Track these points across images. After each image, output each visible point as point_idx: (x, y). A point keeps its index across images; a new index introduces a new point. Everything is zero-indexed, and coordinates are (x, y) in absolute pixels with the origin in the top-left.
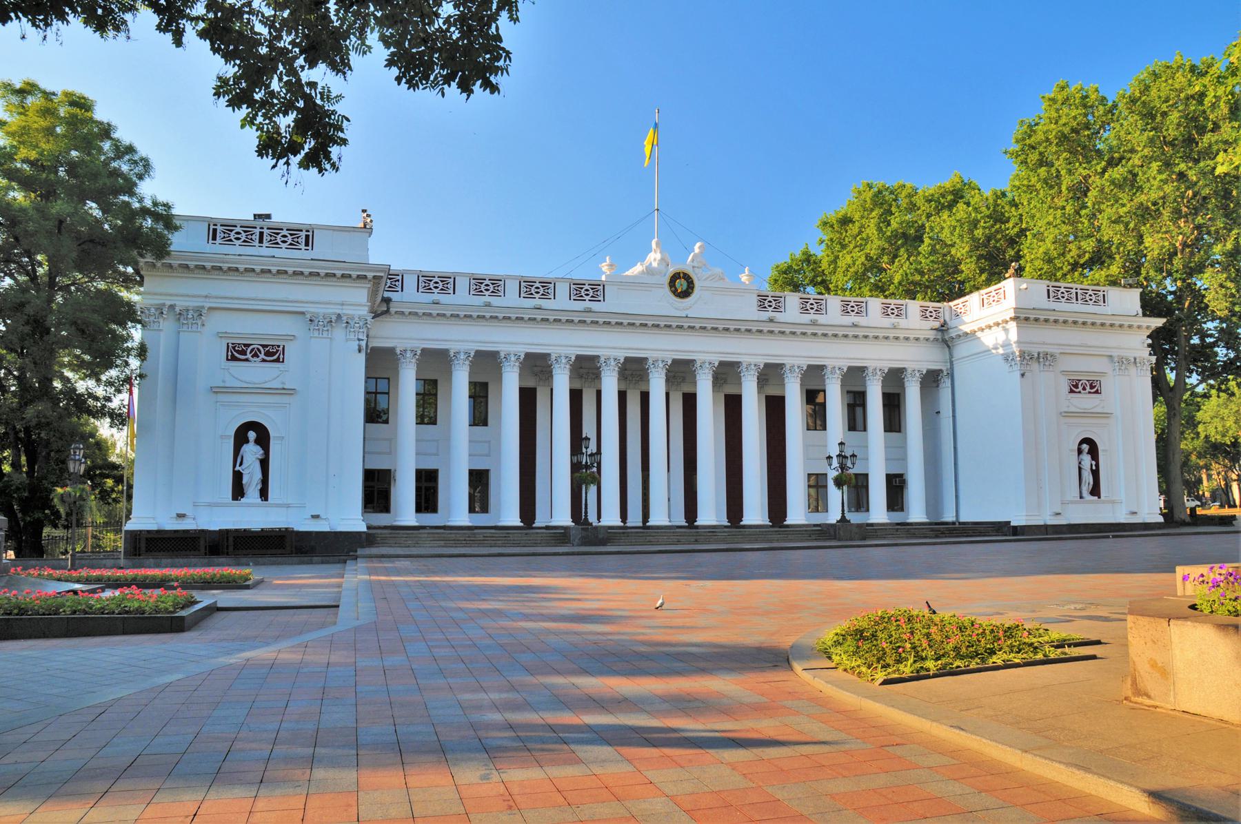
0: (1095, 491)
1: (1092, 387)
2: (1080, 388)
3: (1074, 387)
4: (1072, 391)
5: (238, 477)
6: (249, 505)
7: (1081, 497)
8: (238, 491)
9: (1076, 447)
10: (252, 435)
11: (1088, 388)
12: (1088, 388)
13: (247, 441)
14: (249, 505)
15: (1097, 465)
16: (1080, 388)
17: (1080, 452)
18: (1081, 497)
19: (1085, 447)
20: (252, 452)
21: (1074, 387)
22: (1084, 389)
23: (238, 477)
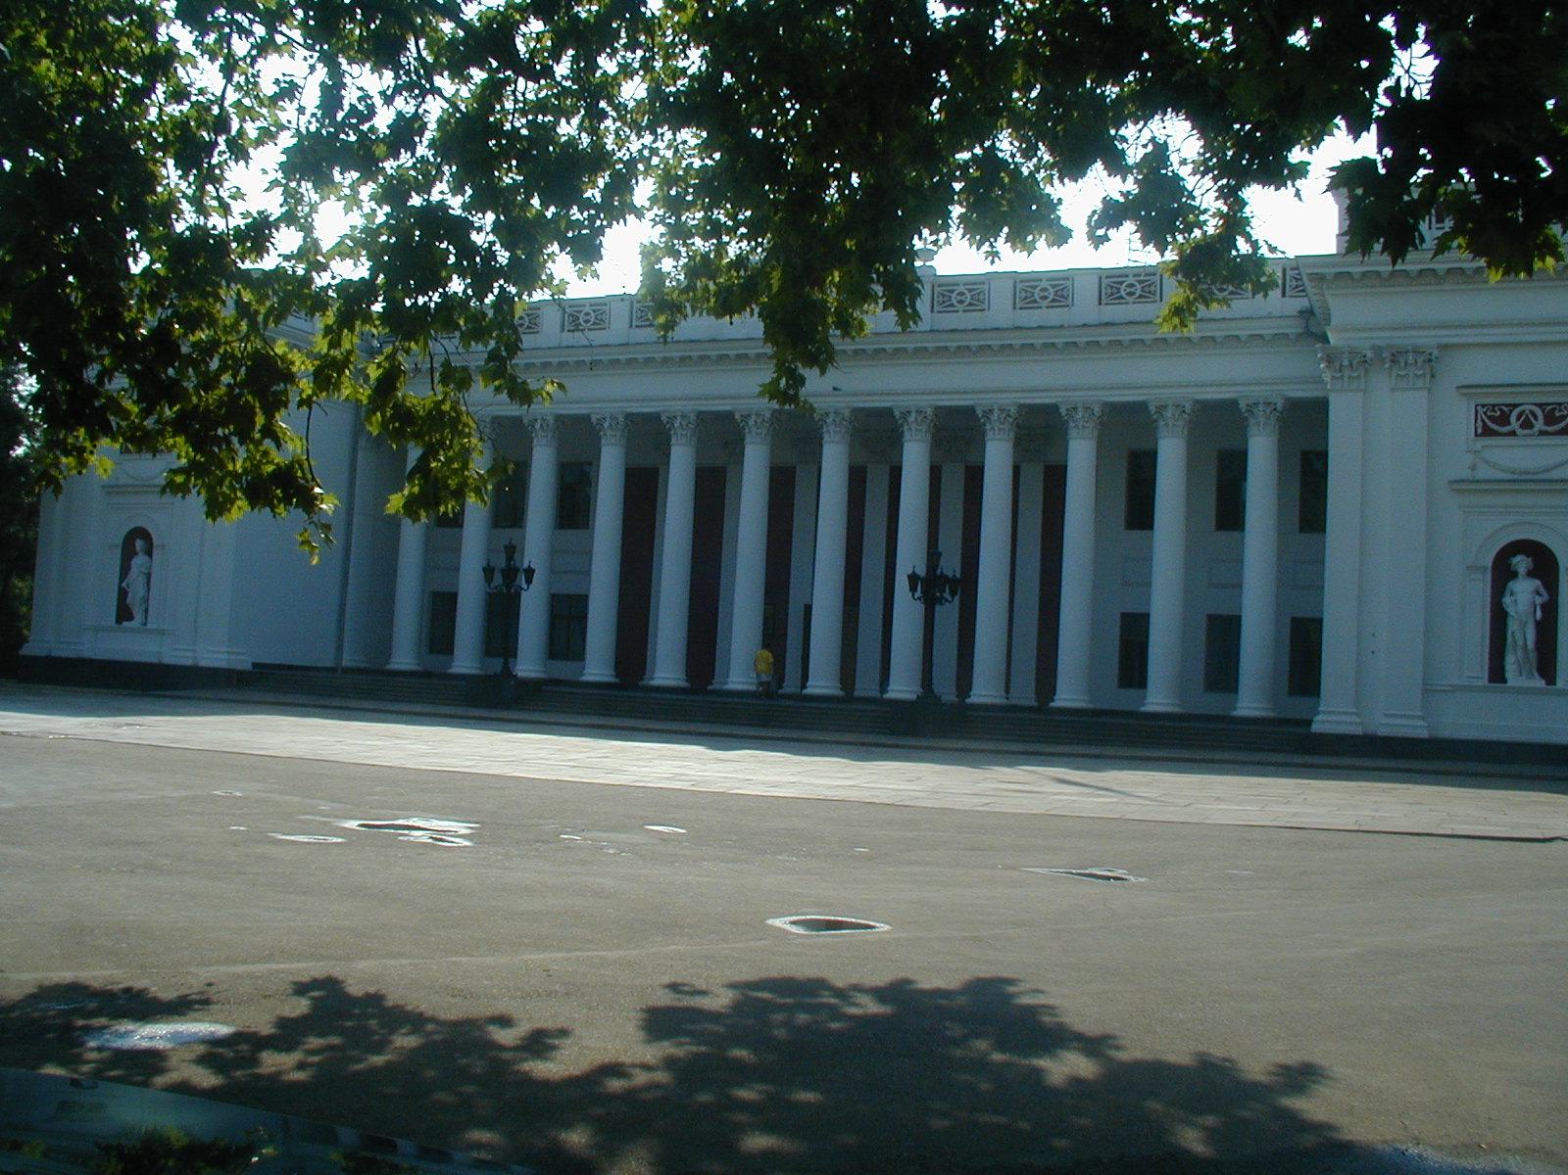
0: (1546, 664)
1: (1550, 419)
2: (1514, 424)
3: (1495, 421)
4: (1487, 432)
5: (123, 594)
6: (132, 630)
7: (1497, 674)
8: (124, 613)
9: (1489, 563)
10: (139, 544)
11: (1539, 425)
12: (1539, 425)
13: (137, 554)
14: (132, 630)
15: (1550, 609)
16: (1514, 424)
17: (1502, 573)
18: (1497, 674)
19: (1521, 563)
20: (139, 562)
21: (1495, 421)
22: (1527, 424)
23: (123, 594)
